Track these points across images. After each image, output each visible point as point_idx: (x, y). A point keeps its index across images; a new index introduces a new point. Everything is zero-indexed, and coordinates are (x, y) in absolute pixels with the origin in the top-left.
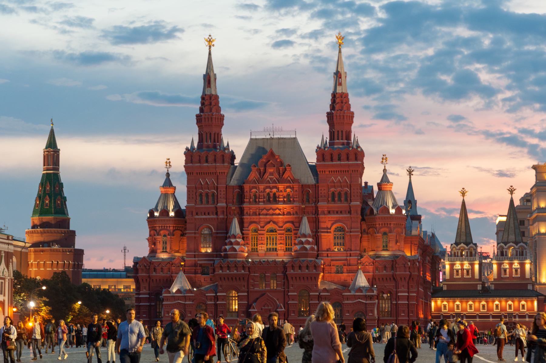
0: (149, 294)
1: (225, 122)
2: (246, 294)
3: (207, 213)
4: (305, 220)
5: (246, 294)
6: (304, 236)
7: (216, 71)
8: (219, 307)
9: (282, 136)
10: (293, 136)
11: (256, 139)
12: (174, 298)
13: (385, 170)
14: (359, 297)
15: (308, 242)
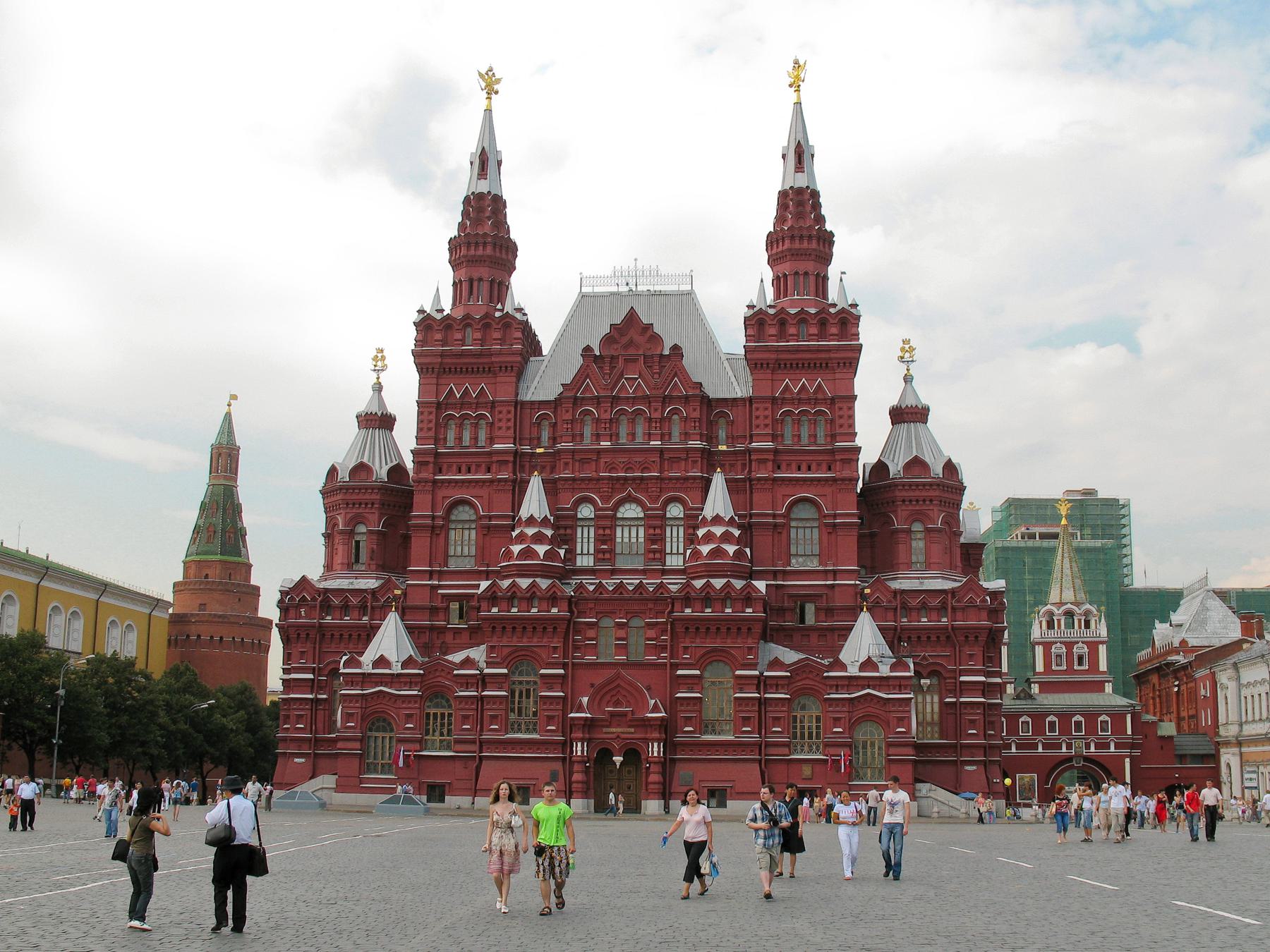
0: (313, 671)
1: (518, 262)
2: (562, 671)
3: (464, 468)
4: (718, 481)
5: (562, 671)
6: (717, 520)
7: (503, 144)
8: (486, 707)
9: (658, 288)
10: (687, 288)
11: (595, 296)
12: (366, 679)
13: (908, 379)
14: (869, 683)
15: (726, 537)
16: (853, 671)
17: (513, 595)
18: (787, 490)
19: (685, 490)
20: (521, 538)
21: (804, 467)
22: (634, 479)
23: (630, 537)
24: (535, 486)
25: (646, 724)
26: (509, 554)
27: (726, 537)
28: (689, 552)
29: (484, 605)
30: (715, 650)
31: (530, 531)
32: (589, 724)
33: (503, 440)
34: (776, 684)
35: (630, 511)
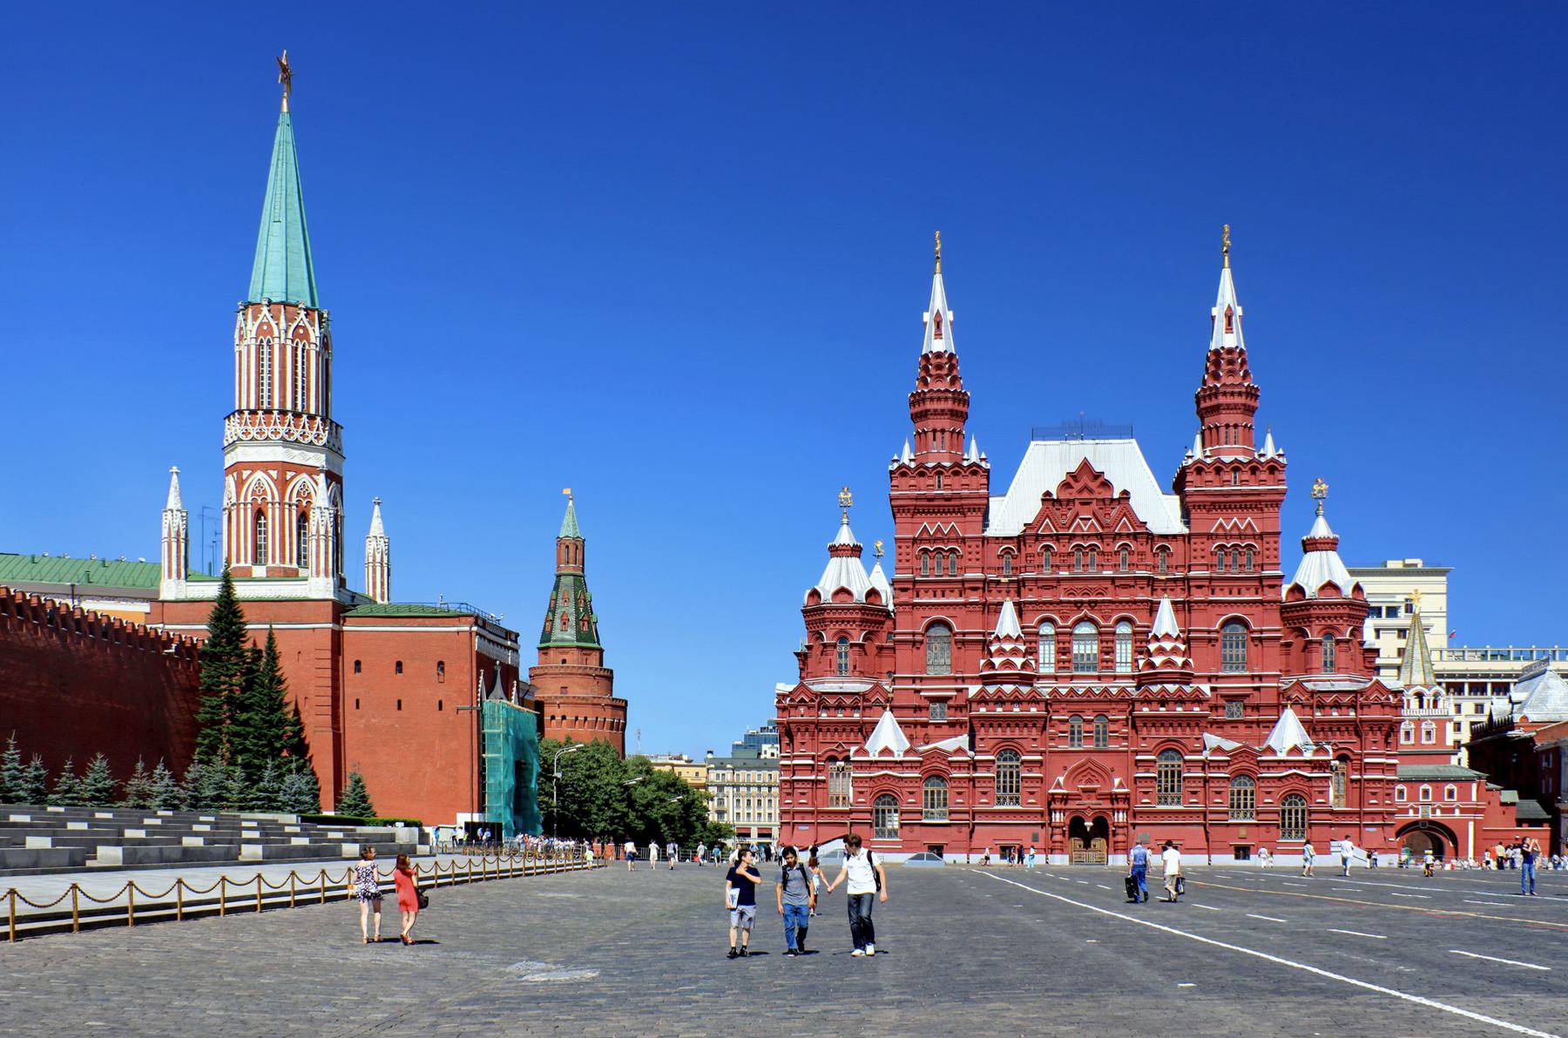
3: (939, 593)
16: (1282, 756)
17: (1000, 701)
18: (1222, 609)
19: (1135, 611)
20: (1001, 652)
21: (1235, 591)
22: (1090, 602)
23: (1086, 648)
24: (1008, 609)
25: (1114, 798)
26: (991, 665)
27: (1175, 650)
28: (1141, 663)
29: (974, 706)
30: (1169, 740)
31: (1008, 647)
32: (1065, 798)
33: (973, 569)
34: (1218, 765)
35: (1086, 629)
